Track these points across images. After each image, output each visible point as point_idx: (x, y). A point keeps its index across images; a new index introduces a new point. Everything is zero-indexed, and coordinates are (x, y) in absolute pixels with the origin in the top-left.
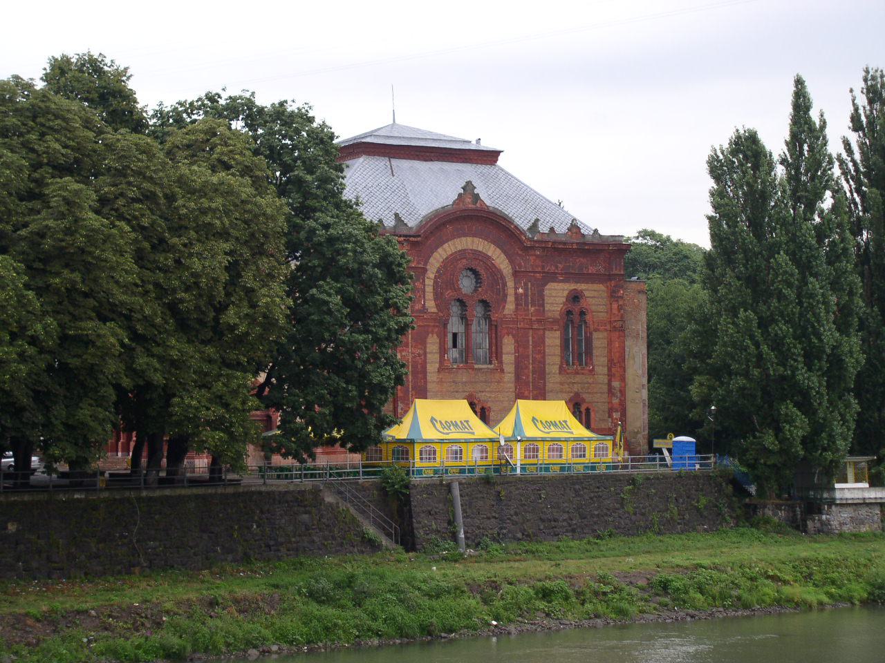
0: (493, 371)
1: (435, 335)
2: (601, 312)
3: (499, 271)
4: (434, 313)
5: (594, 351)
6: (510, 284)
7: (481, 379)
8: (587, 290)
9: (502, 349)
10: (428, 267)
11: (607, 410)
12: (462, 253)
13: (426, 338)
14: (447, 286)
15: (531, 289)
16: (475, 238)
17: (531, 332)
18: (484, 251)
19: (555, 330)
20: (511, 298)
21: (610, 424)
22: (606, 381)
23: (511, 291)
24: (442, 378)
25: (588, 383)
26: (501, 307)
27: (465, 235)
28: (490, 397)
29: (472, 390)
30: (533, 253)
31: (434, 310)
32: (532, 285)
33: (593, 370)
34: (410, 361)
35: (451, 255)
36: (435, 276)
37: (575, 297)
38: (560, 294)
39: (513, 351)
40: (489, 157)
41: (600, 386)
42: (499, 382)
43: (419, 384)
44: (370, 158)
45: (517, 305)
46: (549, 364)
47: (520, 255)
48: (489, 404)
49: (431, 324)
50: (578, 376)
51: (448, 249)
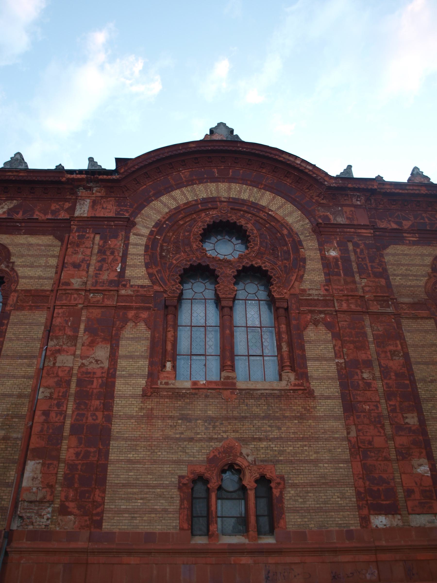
4: (142, 286)
7: (256, 410)
9: (303, 349)
10: (138, 219)
16: (233, 185)
18: (252, 199)
19: (422, 318)
24: (152, 409)
28: (281, 452)
29: (233, 435)
30: (347, 202)
31: (147, 282)
32: (356, 245)
34: (75, 372)
36: (152, 232)
39: (332, 355)
46: (424, 380)
47: (320, 205)
49: (134, 304)
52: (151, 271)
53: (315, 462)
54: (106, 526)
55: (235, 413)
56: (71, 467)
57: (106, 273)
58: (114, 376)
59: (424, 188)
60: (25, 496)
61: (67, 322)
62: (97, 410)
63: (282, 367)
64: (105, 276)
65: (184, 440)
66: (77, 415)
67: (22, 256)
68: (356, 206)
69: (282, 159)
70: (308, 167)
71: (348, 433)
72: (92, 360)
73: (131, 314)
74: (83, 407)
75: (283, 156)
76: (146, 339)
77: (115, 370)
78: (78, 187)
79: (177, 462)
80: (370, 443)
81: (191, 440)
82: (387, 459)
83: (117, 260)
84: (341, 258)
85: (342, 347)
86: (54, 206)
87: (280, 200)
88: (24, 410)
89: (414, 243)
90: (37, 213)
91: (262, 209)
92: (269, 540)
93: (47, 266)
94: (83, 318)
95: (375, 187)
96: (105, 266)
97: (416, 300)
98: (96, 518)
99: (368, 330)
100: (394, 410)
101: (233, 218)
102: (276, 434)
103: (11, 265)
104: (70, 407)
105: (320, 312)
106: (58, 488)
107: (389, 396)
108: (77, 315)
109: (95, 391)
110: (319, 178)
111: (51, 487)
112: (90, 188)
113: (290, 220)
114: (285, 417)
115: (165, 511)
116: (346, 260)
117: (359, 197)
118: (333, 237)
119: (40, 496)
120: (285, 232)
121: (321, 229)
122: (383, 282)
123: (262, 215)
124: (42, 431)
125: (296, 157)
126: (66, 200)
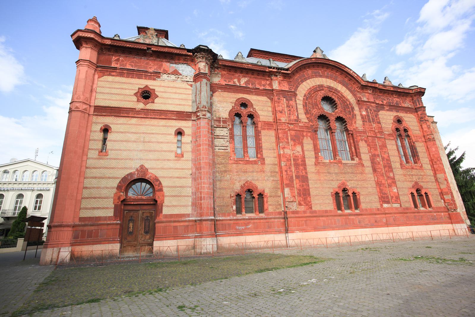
0: (356, 166)
1: (309, 138)
2: (417, 130)
3: (347, 100)
4: (306, 123)
5: (419, 154)
6: (356, 108)
8: (405, 117)
10: (297, 93)
11: (438, 194)
14: (313, 106)
15: (371, 113)
16: (327, 79)
17: (376, 139)
18: (335, 87)
20: (359, 117)
21: (443, 204)
22: (432, 174)
25: (421, 175)
26: (353, 122)
27: (321, 76)
28: (358, 185)
29: (344, 179)
30: (366, 91)
31: (307, 121)
32: (371, 110)
33: (421, 166)
34: (291, 156)
35: (313, 87)
38: (389, 118)
39: (368, 152)
41: (430, 177)
43: (301, 173)
45: (363, 121)
46: (393, 162)
48: (357, 190)
50: (413, 170)
51: (310, 83)
52: (307, 116)
54: (314, 209)
55: (343, 171)
56: (299, 190)
57: (292, 116)
58: (304, 158)
59: (392, 88)
60: (287, 200)
61: (284, 136)
62: (302, 170)
64: (292, 117)
65: (330, 180)
66: (297, 172)
67: (258, 106)
68: (369, 93)
69: (345, 70)
70: (355, 75)
71: (375, 179)
72: (296, 151)
73: (305, 134)
74: (297, 169)
75: (346, 69)
76: (311, 144)
77: (304, 155)
78: (272, 75)
79: (329, 188)
80: (381, 182)
81: (332, 180)
82: (386, 187)
83: (295, 111)
84: (367, 115)
85: (371, 149)
86: (263, 82)
88: (277, 170)
89: (388, 110)
90: (257, 85)
91: (339, 92)
93: (269, 111)
94: (289, 135)
95: (377, 86)
96: (291, 113)
97: (389, 133)
98: (310, 206)
99: (377, 143)
100: (386, 172)
101: (330, 95)
102: (355, 179)
103: (254, 109)
104: (293, 169)
105: (363, 136)
106: (297, 197)
107: (385, 167)
108: (286, 133)
109: (300, 163)
110: (359, 80)
111: (295, 197)
112: (277, 76)
114: (358, 173)
115: (329, 203)
116: (368, 116)
117: (371, 89)
118: (363, 106)
119: (292, 200)
120: (348, 103)
121: (360, 103)
123: (339, 94)
124: (286, 178)
125: (351, 70)
126: (267, 80)
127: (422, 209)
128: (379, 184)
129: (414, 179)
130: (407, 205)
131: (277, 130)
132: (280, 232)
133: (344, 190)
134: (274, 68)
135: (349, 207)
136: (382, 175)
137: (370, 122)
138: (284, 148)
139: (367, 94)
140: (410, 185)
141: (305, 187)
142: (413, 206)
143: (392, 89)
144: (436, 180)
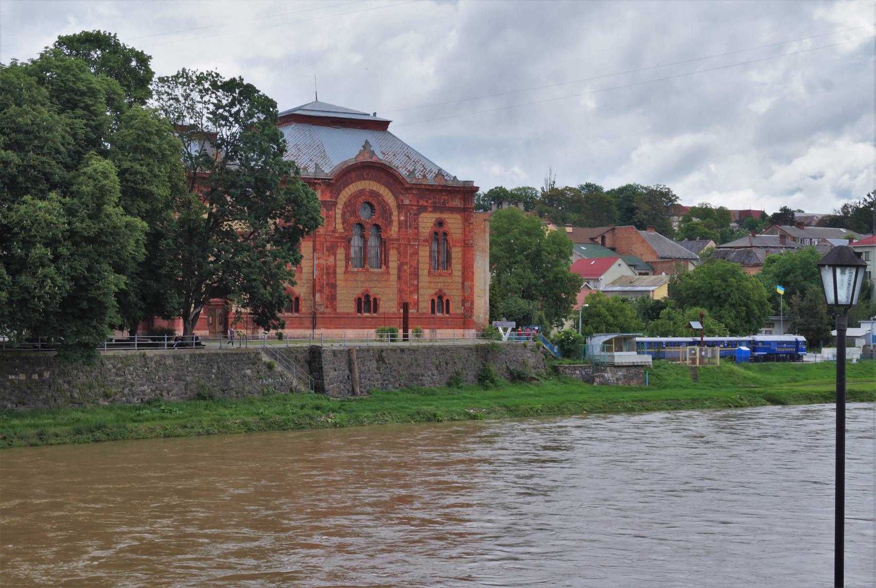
0: (381, 274)
3: (388, 204)
5: (453, 261)
6: (395, 213)
10: (338, 201)
12: (362, 191)
13: (336, 250)
20: (395, 224)
22: (461, 281)
23: (395, 218)
27: (365, 179)
31: (342, 231)
32: (410, 214)
37: (440, 223)
40: (382, 125)
42: (386, 281)
44: (299, 125)
45: (400, 228)
47: (401, 193)
48: (380, 296)
51: (352, 189)
53: (388, 294)
63: (381, 264)
64: (331, 228)
68: (413, 194)
87: (387, 190)
92: (375, 315)
101: (370, 201)
104: (325, 277)
107: (410, 274)
108: (322, 244)
113: (390, 201)
122: (416, 231)
127: (439, 315)
128: (400, 291)
129: (439, 287)
130: (425, 311)
131: (314, 242)
132: (308, 328)
133: (367, 296)
134: (319, 179)
135: (369, 311)
136: (406, 283)
137: (406, 228)
138: (319, 259)
139: (410, 196)
140: (433, 292)
141: (333, 293)
142: (430, 311)
143: (440, 188)
144: (463, 287)
